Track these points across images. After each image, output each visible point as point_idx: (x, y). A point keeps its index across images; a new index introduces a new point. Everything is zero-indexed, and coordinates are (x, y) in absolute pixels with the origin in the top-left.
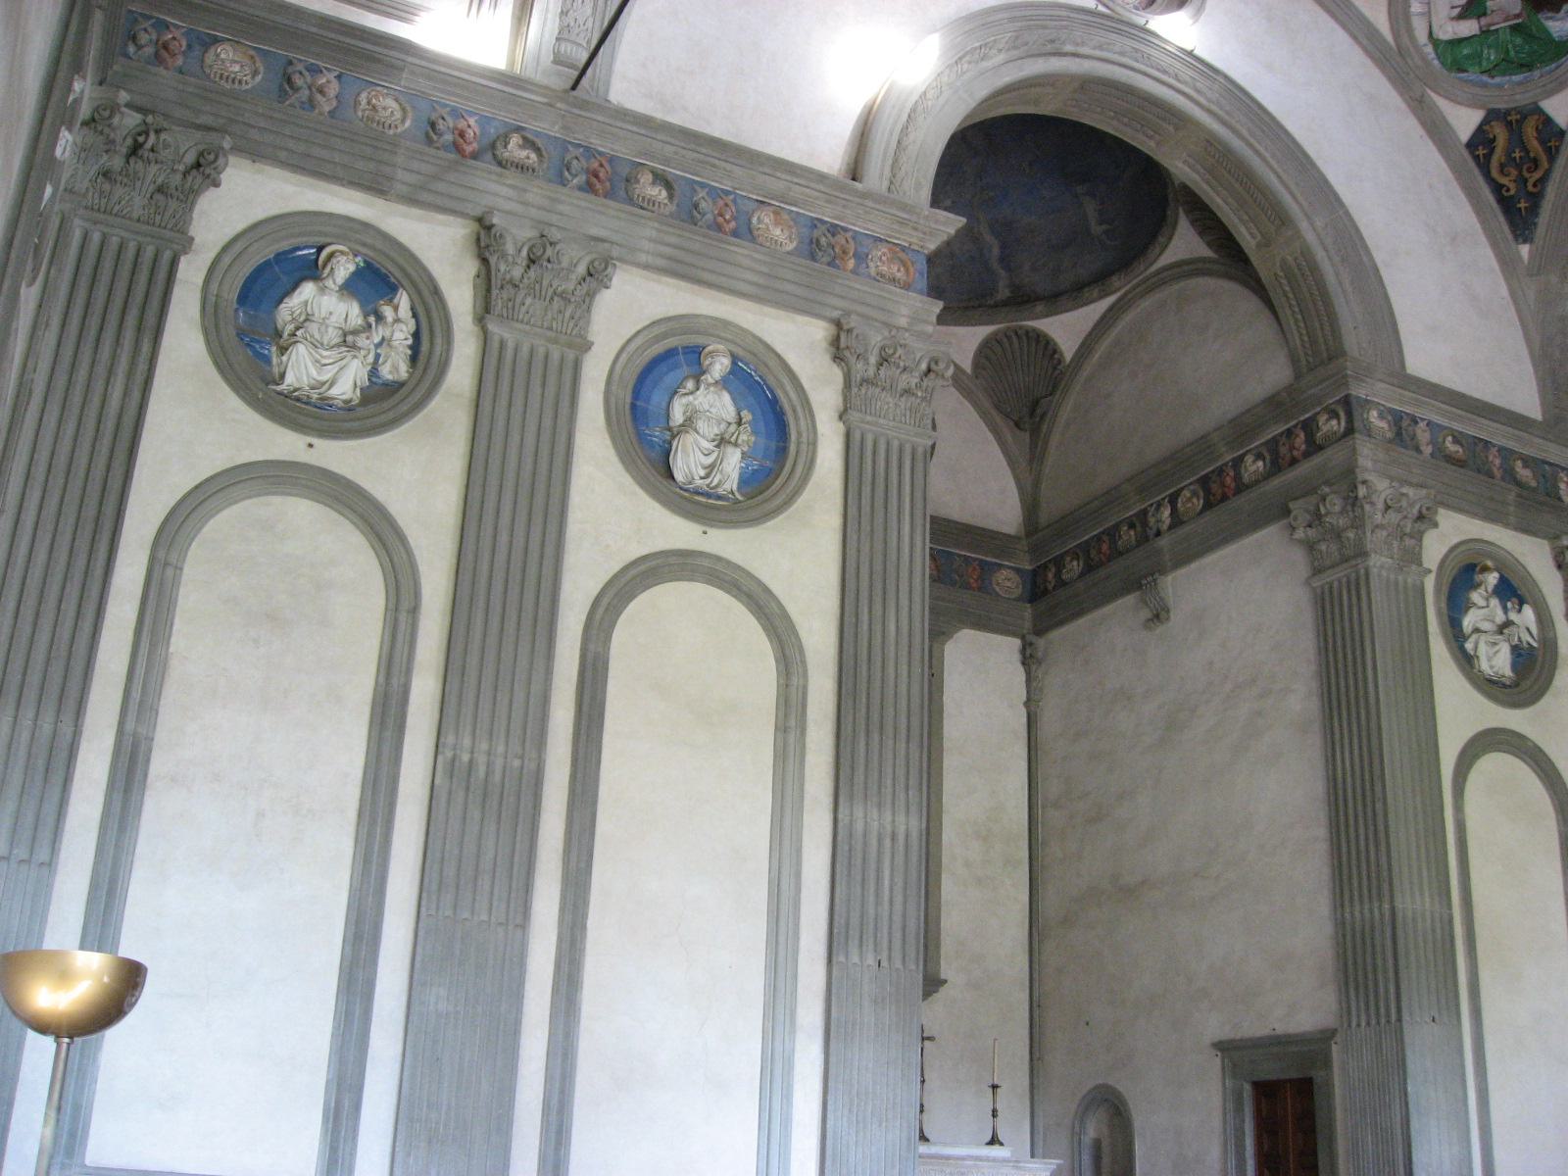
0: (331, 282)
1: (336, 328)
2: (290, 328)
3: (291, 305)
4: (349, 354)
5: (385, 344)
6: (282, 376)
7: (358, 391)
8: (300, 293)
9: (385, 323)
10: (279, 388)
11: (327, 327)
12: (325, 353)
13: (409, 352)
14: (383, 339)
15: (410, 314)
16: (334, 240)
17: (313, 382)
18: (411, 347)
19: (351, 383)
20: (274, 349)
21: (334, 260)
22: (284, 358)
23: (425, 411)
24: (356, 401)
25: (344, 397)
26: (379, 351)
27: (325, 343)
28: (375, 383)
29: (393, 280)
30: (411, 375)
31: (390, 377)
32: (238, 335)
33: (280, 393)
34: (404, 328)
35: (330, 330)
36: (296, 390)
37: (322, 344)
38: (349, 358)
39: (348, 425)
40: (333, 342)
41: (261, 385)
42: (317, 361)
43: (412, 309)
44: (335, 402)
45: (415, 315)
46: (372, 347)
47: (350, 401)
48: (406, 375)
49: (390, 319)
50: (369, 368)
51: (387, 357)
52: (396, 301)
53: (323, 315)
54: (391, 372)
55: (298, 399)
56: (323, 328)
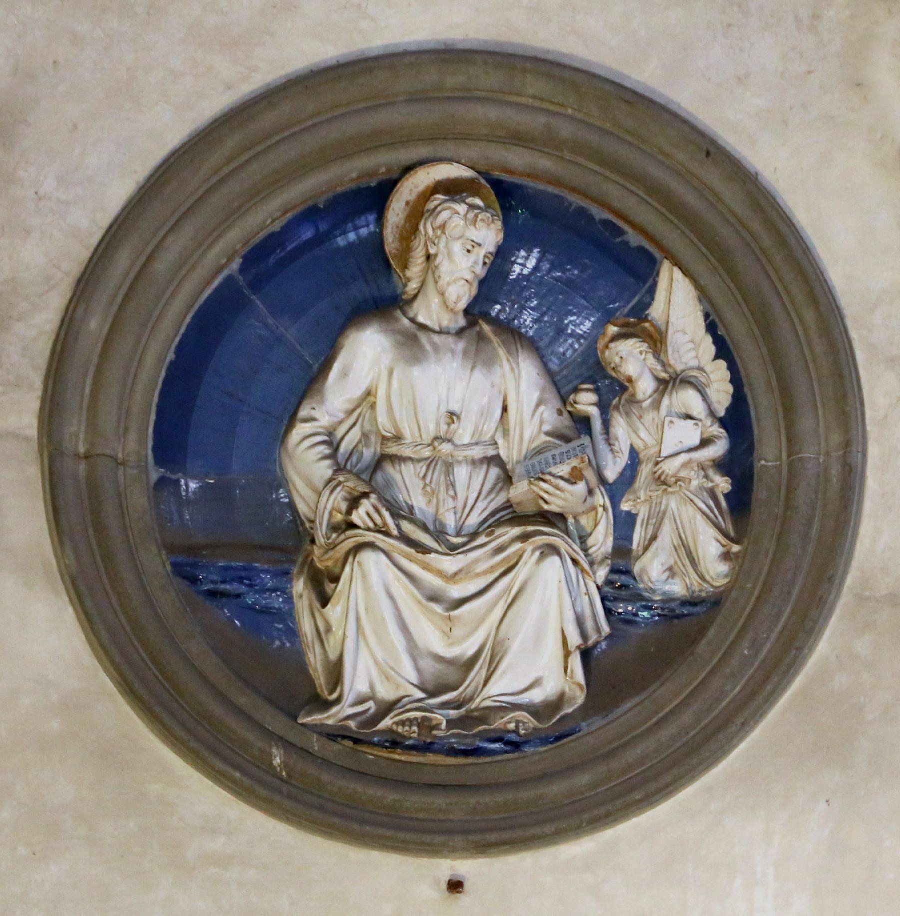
0: (435, 300)
1: (475, 463)
2: (337, 500)
3: (325, 420)
4: (529, 546)
5: (645, 471)
6: (336, 673)
7: (576, 662)
8: (345, 374)
9: (634, 401)
10: (330, 718)
11: (449, 467)
12: (450, 564)
13: (723, 484)
14: (634, 454)
15: (708, 347)
16: (424, 151)
17: (429, 666)
18: (723, 466)
19: (552, 649)
20: (300, 587)
21: (427, 227)
22: (334, 611)
23: (798, 683)
24: (580, 698)
25: (537, 696)
26: (625, 507)
27: (450, 521)
28: (629, 621)
29: (634, 238)
30: (737, 578)
31: (677, 588)
32: (179, 569)
33: (335, 735)
34: (690, 399)
35: (462, 473)
36: (387, 708)
37: (439, 533)
38: (530, 559)
39: (556, 789)
40: (474, 520)
41: (277, 723)
42: (434, 598)
43: (711, 328)
44: (506, 722)
45: (723, 350)
46: (601, 499)
47: (560, 701)
48: (723, 568)
49: (645, 386)
50: (602, 573)
51: (658, 519)
52: (656, 311)
53: (430, 430)
54: (672, 572)
55: (395, 742)
56: (438, 475)
